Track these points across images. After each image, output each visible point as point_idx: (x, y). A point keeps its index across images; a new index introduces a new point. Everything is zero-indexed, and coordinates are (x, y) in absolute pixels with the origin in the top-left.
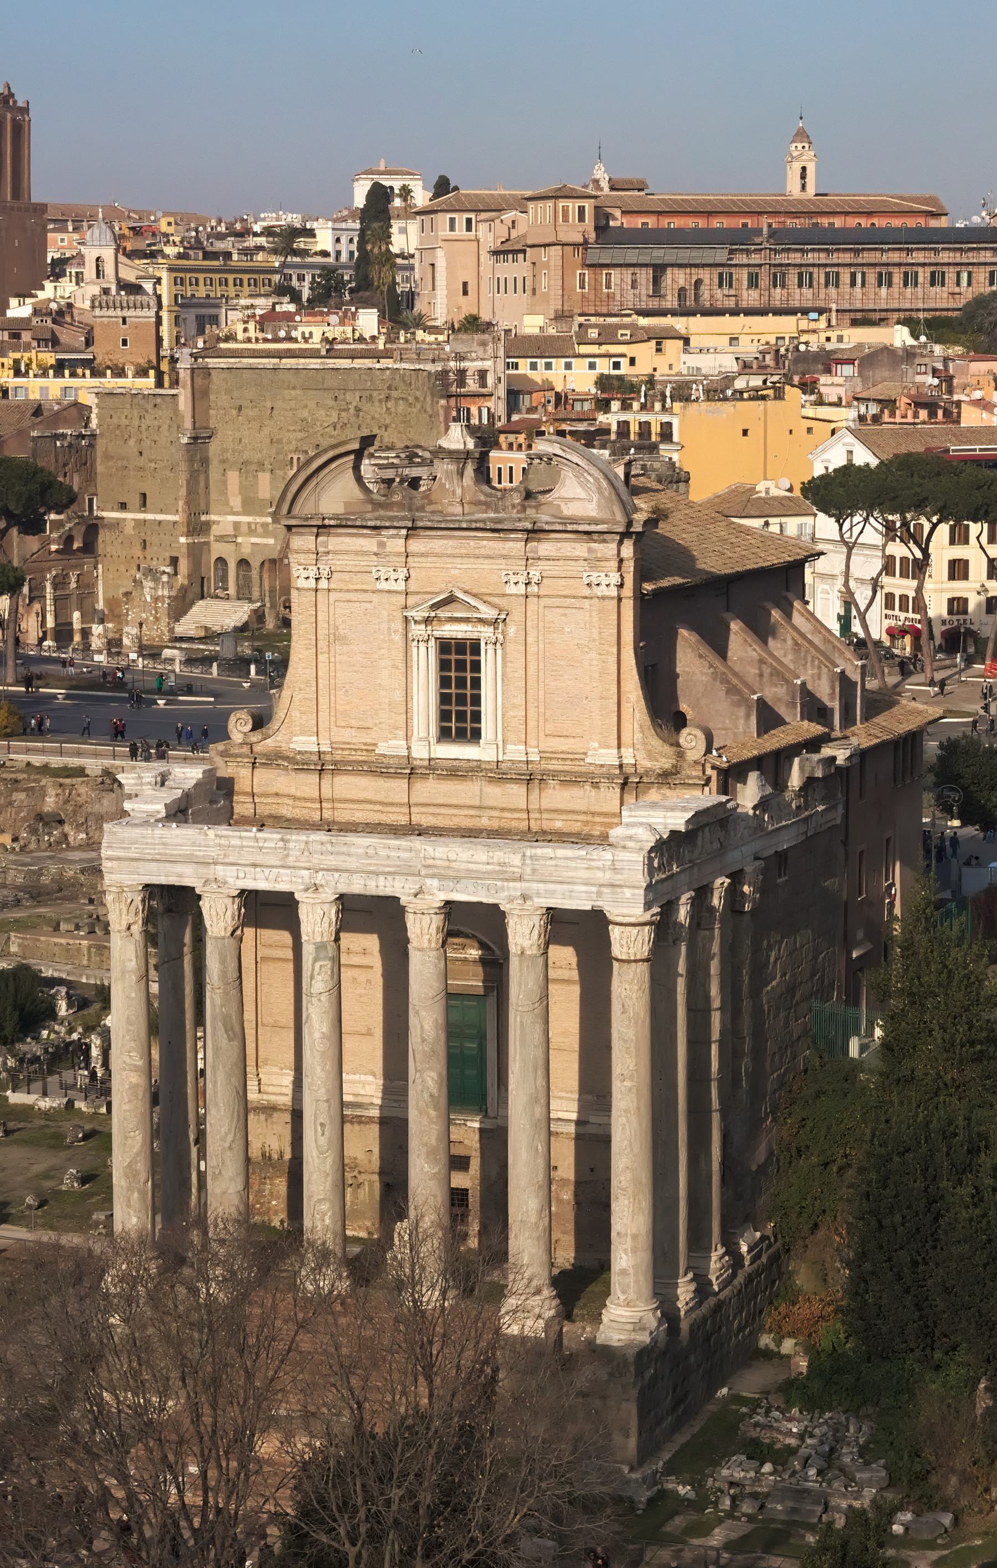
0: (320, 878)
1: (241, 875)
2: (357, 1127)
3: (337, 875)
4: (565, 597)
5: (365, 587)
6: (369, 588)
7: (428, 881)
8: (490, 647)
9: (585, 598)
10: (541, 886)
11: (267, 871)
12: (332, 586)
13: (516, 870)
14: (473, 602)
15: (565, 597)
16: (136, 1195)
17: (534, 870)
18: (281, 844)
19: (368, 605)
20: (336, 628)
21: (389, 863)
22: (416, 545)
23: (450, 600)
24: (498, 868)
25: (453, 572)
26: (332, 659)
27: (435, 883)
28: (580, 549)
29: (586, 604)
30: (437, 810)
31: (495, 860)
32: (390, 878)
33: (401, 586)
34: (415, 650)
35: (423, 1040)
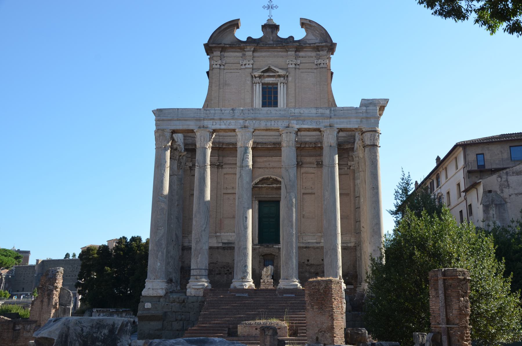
0: (247, 124)
1: (214, 124)
2: (229, 251)
3: (254, 121)
7: (292, 122)
8: (282, 84)
10: (338, 120)
11: (225, 122)
14: (277, 69)
16: (160, 253)
17: (335, 115)
19: (238, 74)
22: (256, 54)
27: (295, 122)
28: (313, 54)
29: (315, 71)
30: (262, 137)
31: (319, 112)
32: (276, 121)
33: (251, 66)
34: (255, 87)
35: (290, 181)
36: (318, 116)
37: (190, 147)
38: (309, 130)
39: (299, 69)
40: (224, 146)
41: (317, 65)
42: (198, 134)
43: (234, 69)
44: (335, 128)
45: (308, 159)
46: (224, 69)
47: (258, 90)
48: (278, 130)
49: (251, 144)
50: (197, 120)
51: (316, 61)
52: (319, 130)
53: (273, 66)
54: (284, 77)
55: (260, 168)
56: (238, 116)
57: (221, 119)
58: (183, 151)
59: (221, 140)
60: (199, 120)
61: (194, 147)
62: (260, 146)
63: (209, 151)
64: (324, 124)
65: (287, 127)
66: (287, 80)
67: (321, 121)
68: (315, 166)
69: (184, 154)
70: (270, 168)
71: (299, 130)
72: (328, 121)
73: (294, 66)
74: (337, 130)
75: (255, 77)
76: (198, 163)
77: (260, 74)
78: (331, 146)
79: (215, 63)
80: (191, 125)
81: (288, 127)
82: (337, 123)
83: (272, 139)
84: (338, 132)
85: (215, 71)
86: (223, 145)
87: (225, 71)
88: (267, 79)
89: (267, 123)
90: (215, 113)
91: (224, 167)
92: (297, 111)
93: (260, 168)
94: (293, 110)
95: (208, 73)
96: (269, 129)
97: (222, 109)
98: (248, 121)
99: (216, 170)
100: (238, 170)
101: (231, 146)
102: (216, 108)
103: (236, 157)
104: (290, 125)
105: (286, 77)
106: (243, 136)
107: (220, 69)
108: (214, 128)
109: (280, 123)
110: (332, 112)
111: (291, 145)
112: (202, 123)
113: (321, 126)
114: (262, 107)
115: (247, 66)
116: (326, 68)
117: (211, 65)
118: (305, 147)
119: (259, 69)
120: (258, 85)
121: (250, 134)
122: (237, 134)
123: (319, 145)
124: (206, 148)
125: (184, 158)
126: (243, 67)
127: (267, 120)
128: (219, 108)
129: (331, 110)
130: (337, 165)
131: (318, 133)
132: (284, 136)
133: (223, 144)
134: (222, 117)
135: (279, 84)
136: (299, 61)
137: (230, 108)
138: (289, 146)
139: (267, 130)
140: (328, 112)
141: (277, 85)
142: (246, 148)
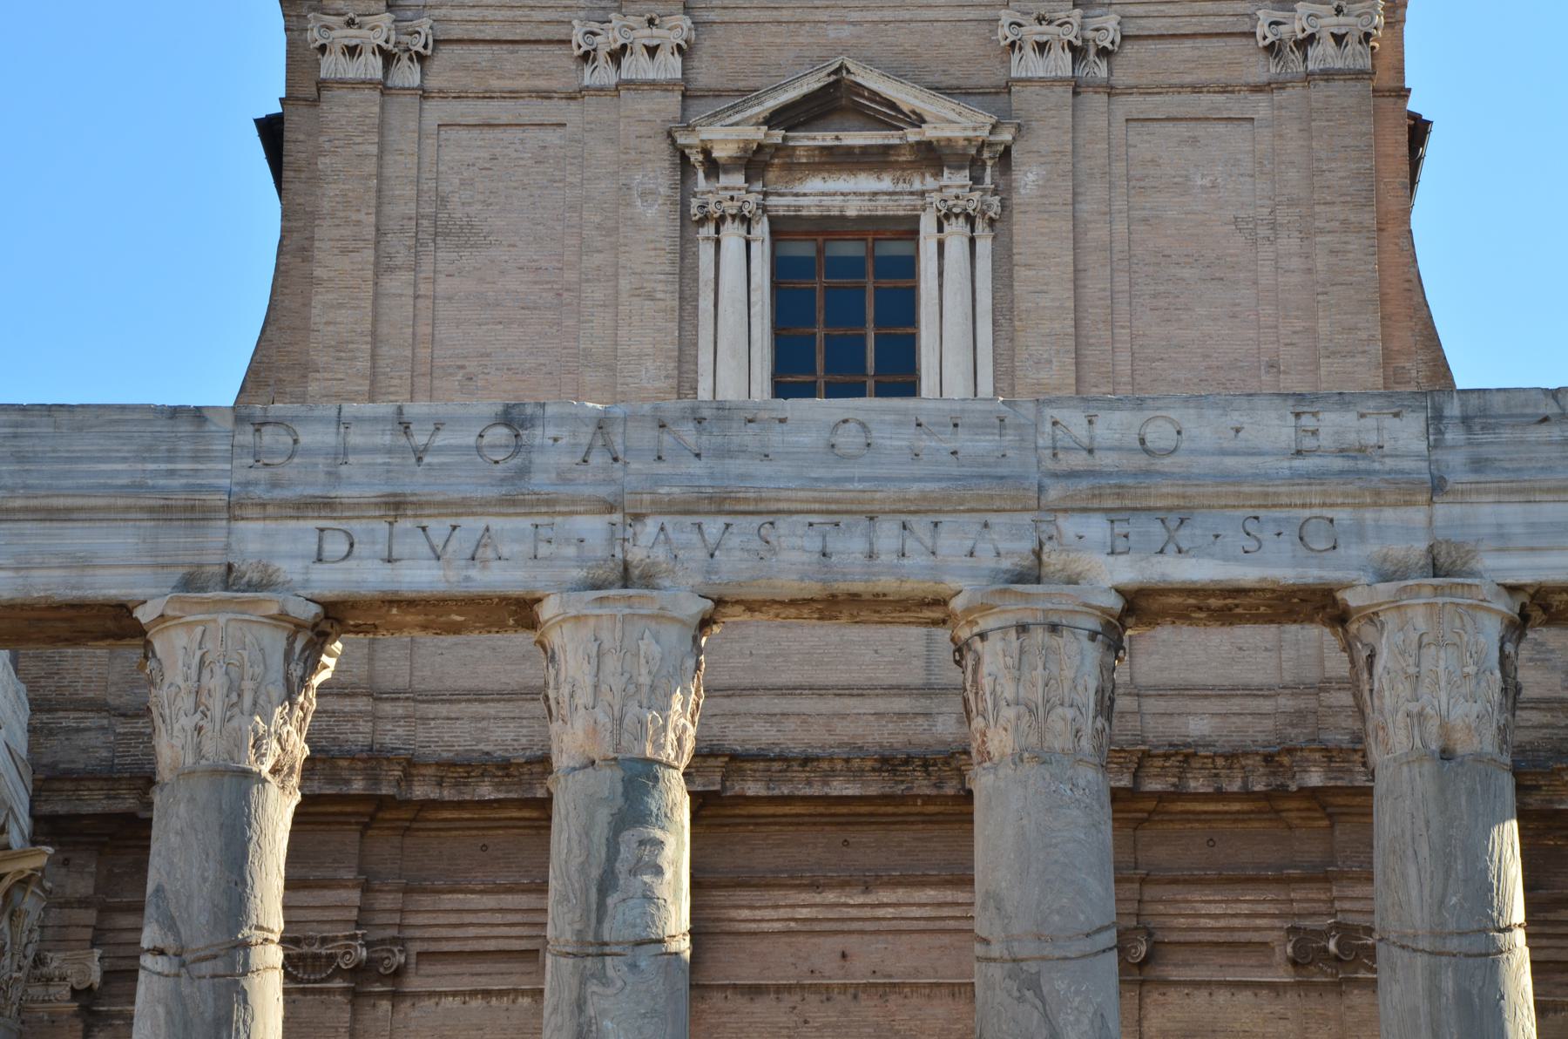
0: (645, 545)
3: (713, 526)
4: (1196, 89)
5: (541, 83)
6: (554, 84)
7: (1069, 526)
8: (956, 229)
9: (1257, 89)
10: (1513, 513)
11: (438, 527)
12: (433, 83)
13: (1408, 464)
15: (1196, 89)
17: (1478, 464)
18: (501, 434)
19: (552, 137)
20: (442, 201)
21: (918, 470)
23: (835, 100)
24: (1338, 463)
25: (832, 32)
26: (424, 289)
27: (1096, 528)
29: (1261, 106)
31: (1326, 440)
32: (920, 524)
33: (669, 67)
34: (706, 253)
36: (1313, 477)
37: (95, 802)
38: (1225, 606)
39: (1111, 90)
40: (420, 791)
41: (1273, 49)
42: (175, 649)
43: (514, 95)
44: (1486, 589)
45: (1210, 910)
46: (424, 94)
47: (739, 274)
48: (930, 608)
49: (678, 729)
50: (165, 513)
51: (1264, 16)
52: (1321, 605)
53: (870, 62)
54: (975, 165)
55: (755, 991)
56: (563, 478)
57: (395, 506)
58: (15, 838)
59: (393, 735)
60: (189, 512)
61: (127, 803)
62: (753, 788)
63: (278, 811)
64: (1373, 548)
65: (1021, 577)
66: (1004, 192)
67: (1342, 515)
68: (1283, 975)
69: (27, 865)
70: (855, 991)
71: (1139, 606)
72: (1417, 515)
73: (1061, 63)
74: (1506, 606)
75: (713, 167)
76: (169, 924)
77: (759, 134)
78: (1446, 754)
79: (343, 36)
80: (112, 562)
81: (1031, 574)
82: (1503, 542)
83: (870, 726)
84: (1518, 626)
85: (348, 113)
86: (407, 778)
87: (435, 112)
88: (815, 184)
89: (836, 544)
90: (342, 453)
91: (413, 983)
92: (1115, 427)
93: (755, 991)
94: (1074, 420)
95: (271, 131)
96: (854, 598)
97: (414, 409)
98: (651, 526)
99: (339, 1013)
100: (557, 974)
101: (486, 791)
102: (350, 409)
103: (542, 888)
104: (1053, 559)
105: (989, 161)
106: (611, 663)
107: (384, 89)
108: (330, 593)
109: (954, 539)
110: (1453, 435)
111: (1060, 740)
112: (212, 545)
113: (1347, 567)
114: (781, 390)
115: (637, 67)
116: (1358, 75)
117: (301, 59)
118: (1178, 795)
119: (746, 95)
120: (732, 237)
121: (674, 637)
122: (555, 638)
123: (1315, 779)
124: (248, 778)
125: (31, 904)
126: (603, 74)
127: (835, 512)
128: (384, 408)
129: (1437, 419)
130: (1519, 936)
131: (1310, 643)
132: (994, 657)
133: (411, 765)
134: (414, 483)
135: (927, 225)
136: (1111, 21)
137: (489, 407)
138: (1042, 757)
139: (833, 605)
140: (1408, 433)
141: (909, 230)
142: (640, 776)
